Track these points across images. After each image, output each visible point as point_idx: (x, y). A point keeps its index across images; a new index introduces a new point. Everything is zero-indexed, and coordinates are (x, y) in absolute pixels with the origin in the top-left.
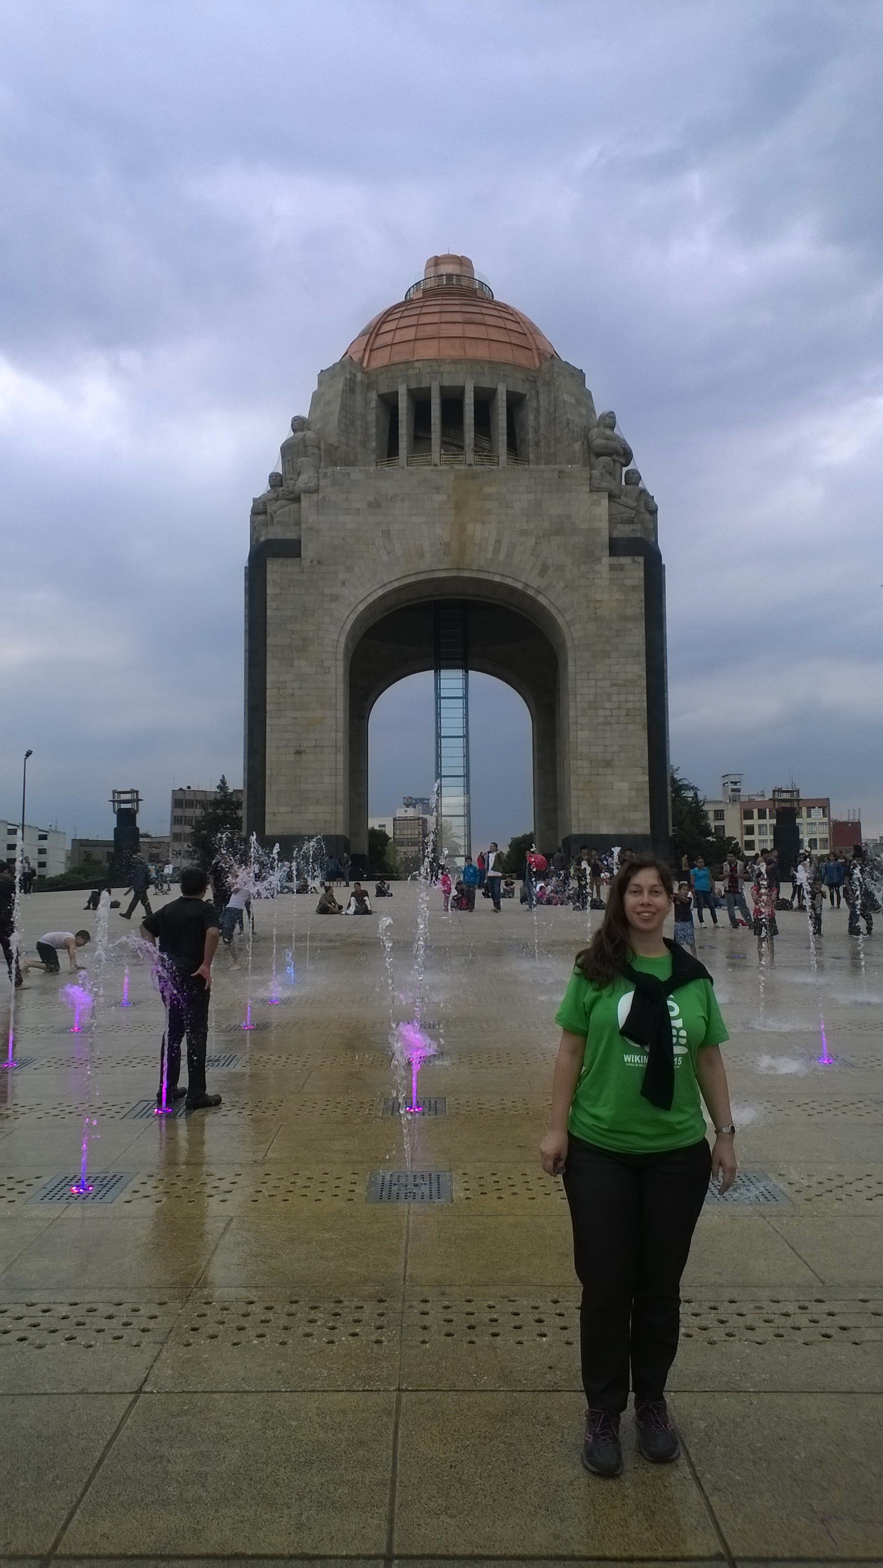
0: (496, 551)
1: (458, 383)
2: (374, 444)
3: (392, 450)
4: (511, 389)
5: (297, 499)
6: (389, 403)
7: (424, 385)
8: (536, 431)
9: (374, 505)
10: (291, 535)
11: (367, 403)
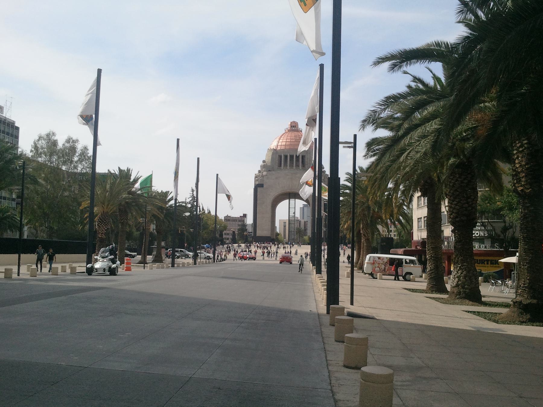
0: (298, 187)
1: (293, 154)
2: (277, 164)
3: (280, 165)
4: (303, 155)
6: (280, 157)
7: (287, 154)
8: (307, 162)
9: (276, 178)
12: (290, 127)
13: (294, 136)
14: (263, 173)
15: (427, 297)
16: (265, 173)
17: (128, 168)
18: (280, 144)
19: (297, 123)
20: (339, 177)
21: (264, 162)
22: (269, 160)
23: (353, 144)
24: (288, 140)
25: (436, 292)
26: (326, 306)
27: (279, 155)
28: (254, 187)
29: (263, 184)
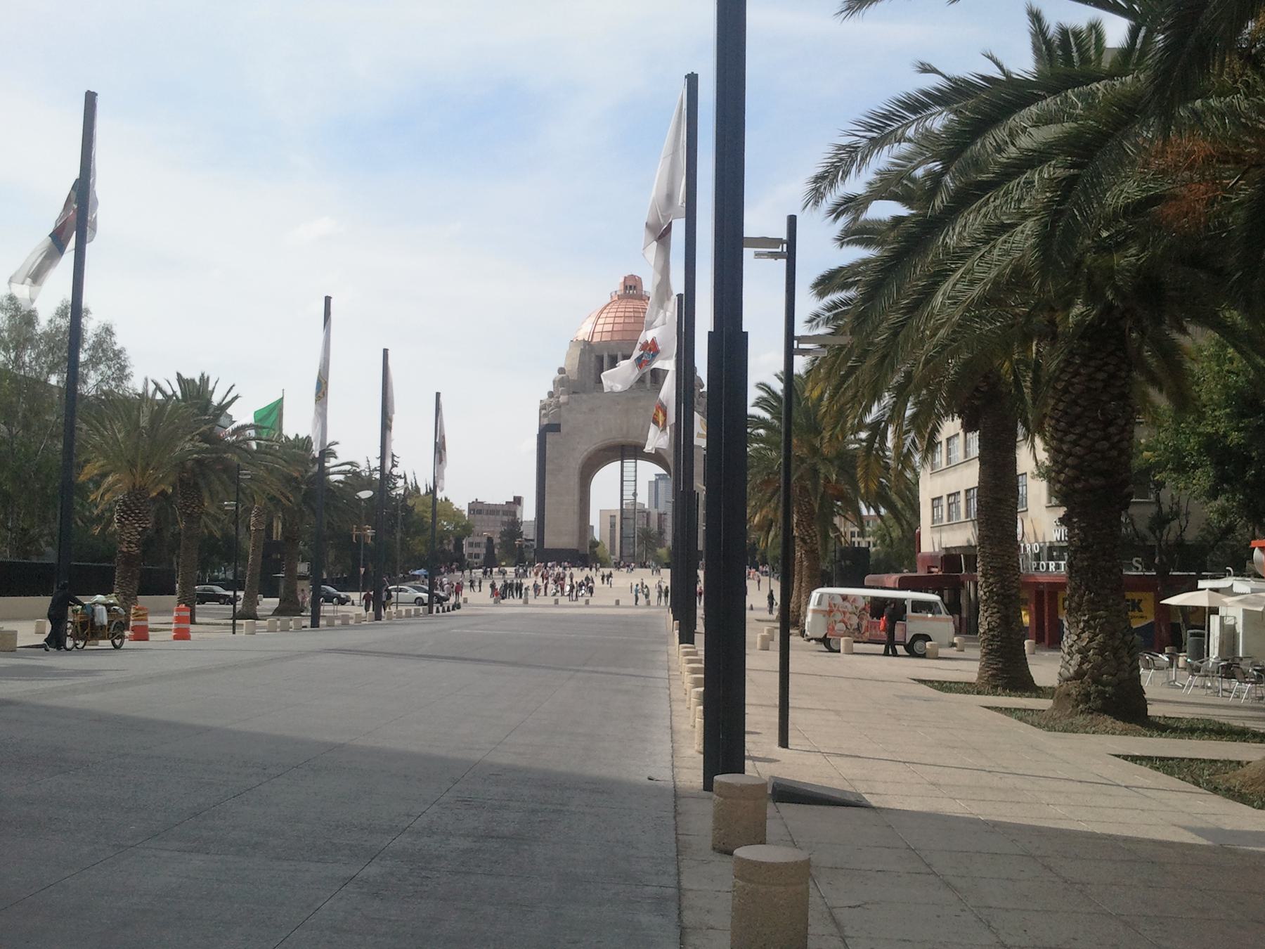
5: (560, 407)
9: (592, 410)
10: (556, 422)
11: (590, 359)
12: (622, 288)
13: (632, 310)
14: (558, 397)
15: (988, 708)
16: (563, 399)
17: (203, 375)
18: (599, 328)
19: (640, 278)
20: (744, 330)
21: (561, 371)
22: (572, 366)
23: (785, 246)
24: (617, 320)
25: (1004, 689)
26: (702, 756)
27: (597, 356)
28: (536, 431)
29: (560, 425)
